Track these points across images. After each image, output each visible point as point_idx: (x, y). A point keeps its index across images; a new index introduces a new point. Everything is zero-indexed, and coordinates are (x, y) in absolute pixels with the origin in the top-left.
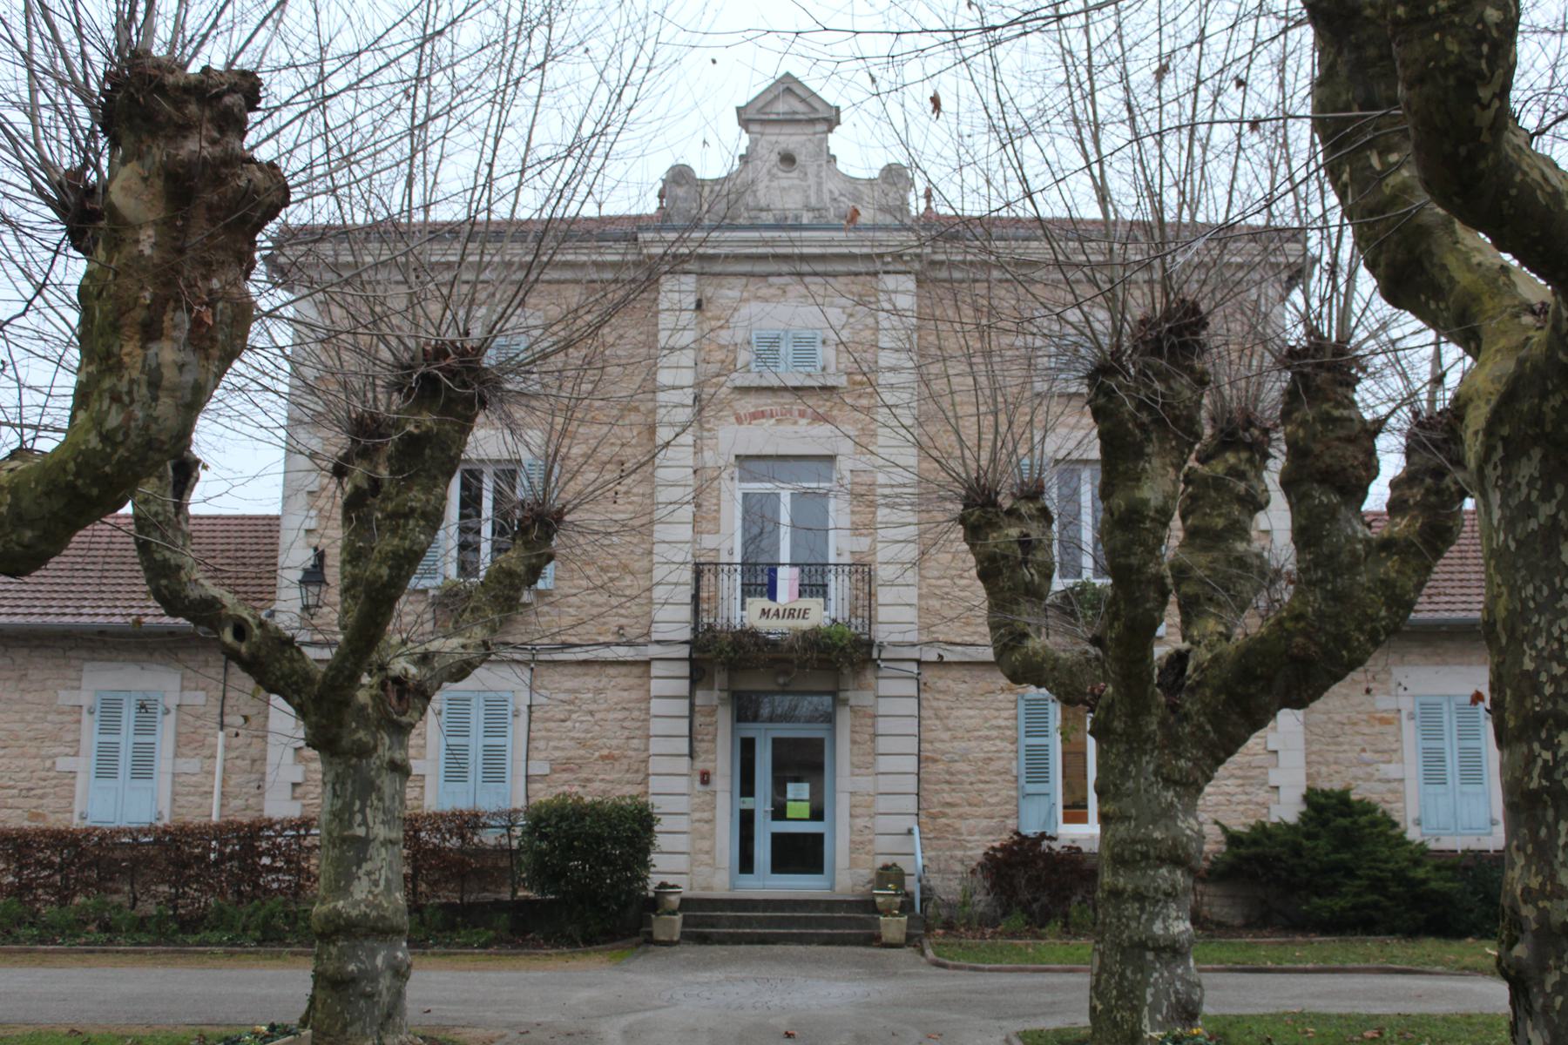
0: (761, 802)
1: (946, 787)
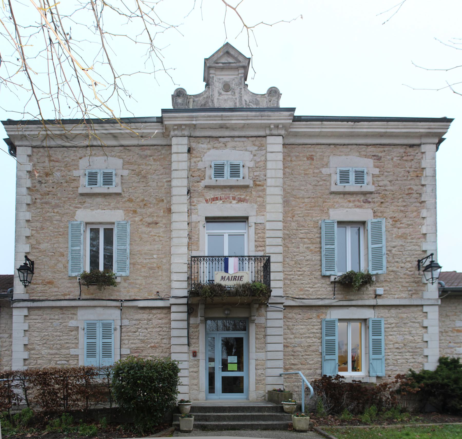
0: (218, 365)
1: (292, 357)
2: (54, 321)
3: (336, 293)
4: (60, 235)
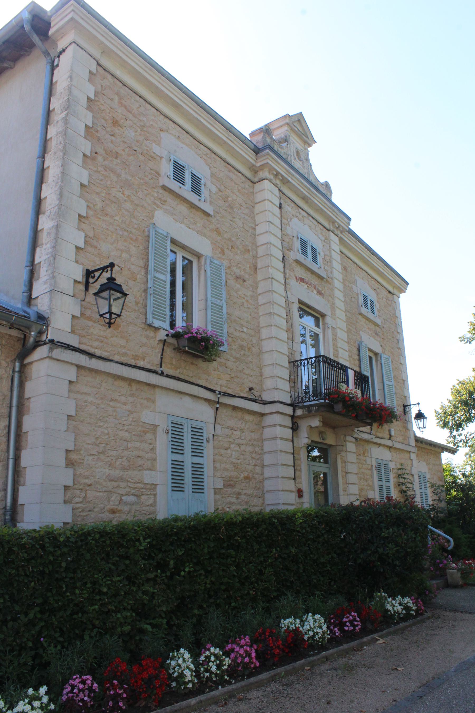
2: (119, 405)
4: (132, 239)
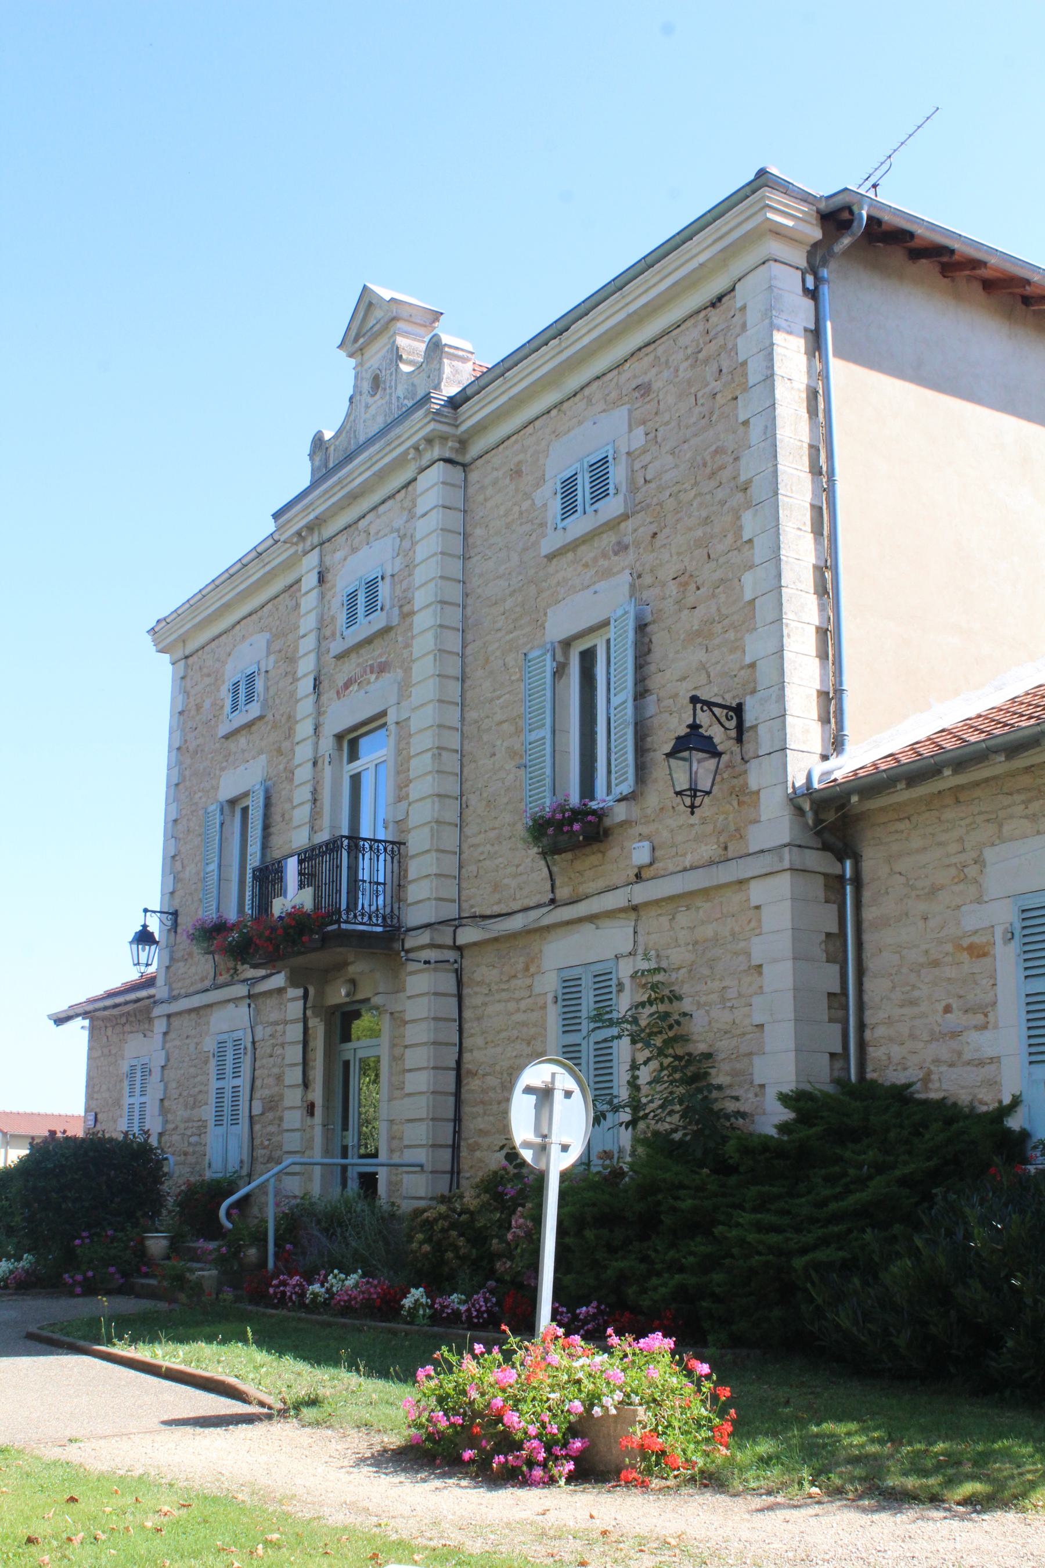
3: (558, 883)
